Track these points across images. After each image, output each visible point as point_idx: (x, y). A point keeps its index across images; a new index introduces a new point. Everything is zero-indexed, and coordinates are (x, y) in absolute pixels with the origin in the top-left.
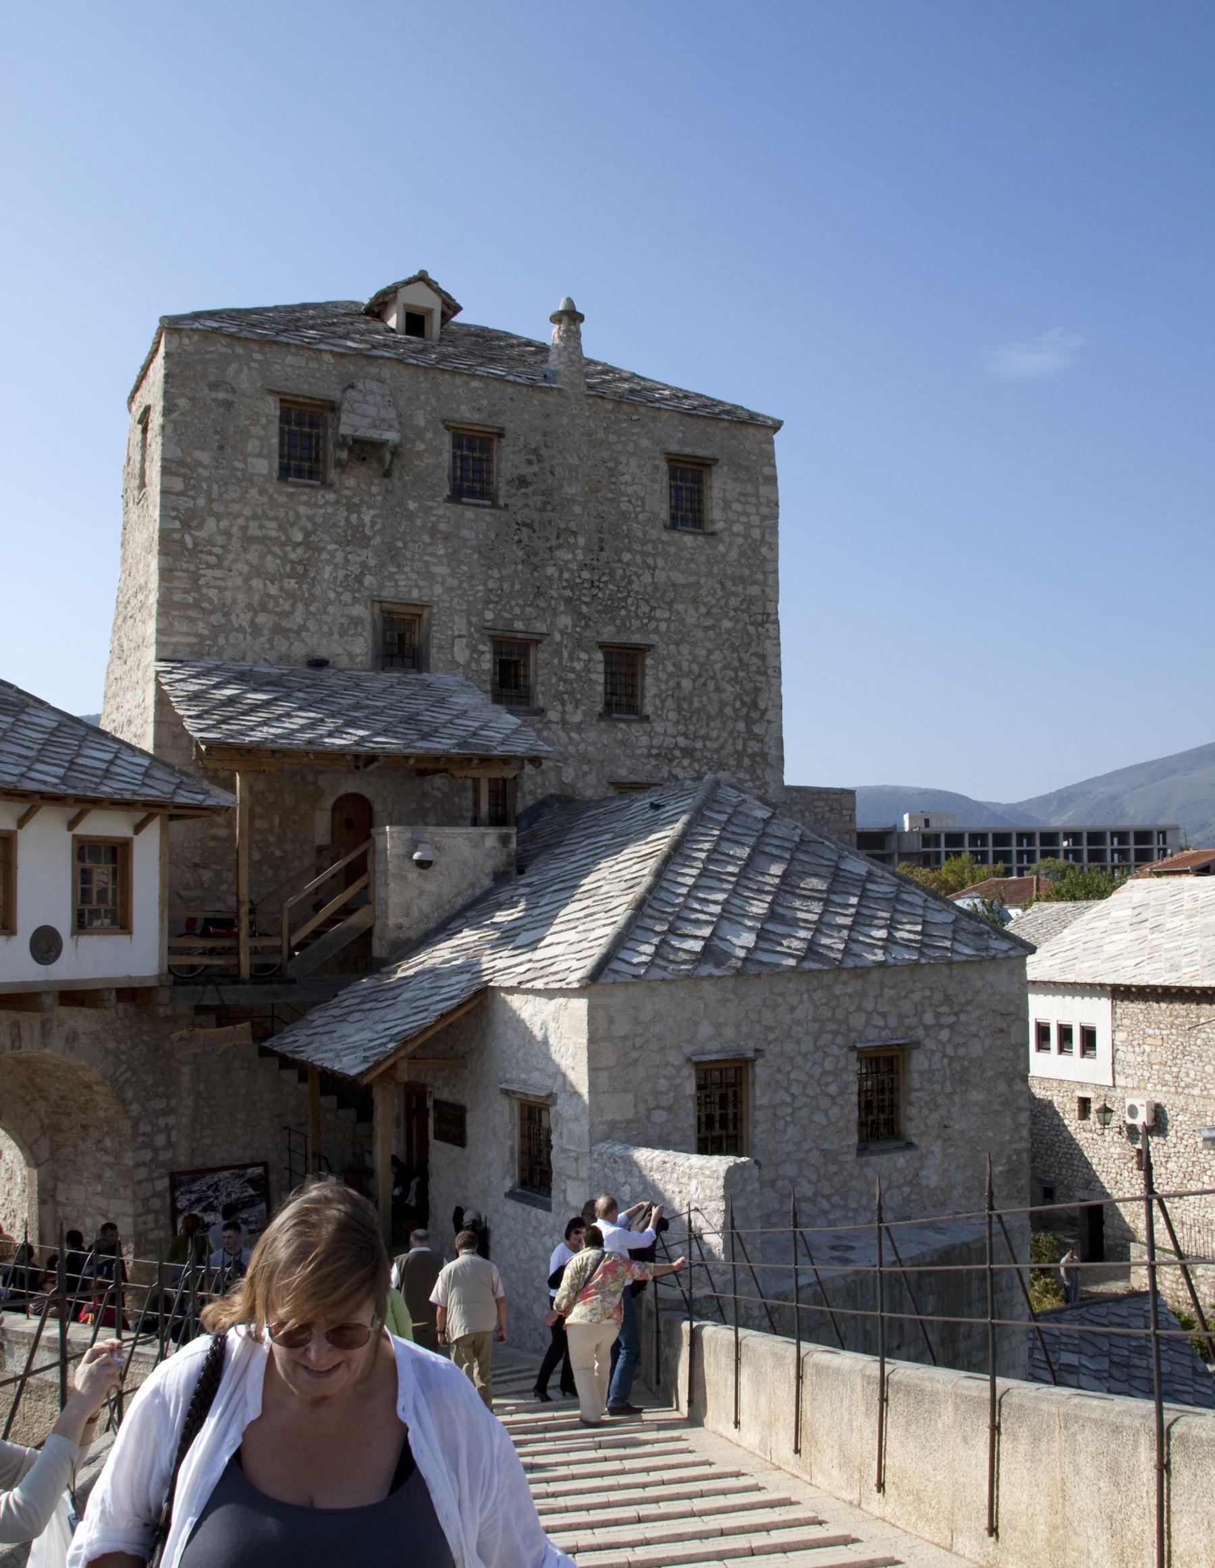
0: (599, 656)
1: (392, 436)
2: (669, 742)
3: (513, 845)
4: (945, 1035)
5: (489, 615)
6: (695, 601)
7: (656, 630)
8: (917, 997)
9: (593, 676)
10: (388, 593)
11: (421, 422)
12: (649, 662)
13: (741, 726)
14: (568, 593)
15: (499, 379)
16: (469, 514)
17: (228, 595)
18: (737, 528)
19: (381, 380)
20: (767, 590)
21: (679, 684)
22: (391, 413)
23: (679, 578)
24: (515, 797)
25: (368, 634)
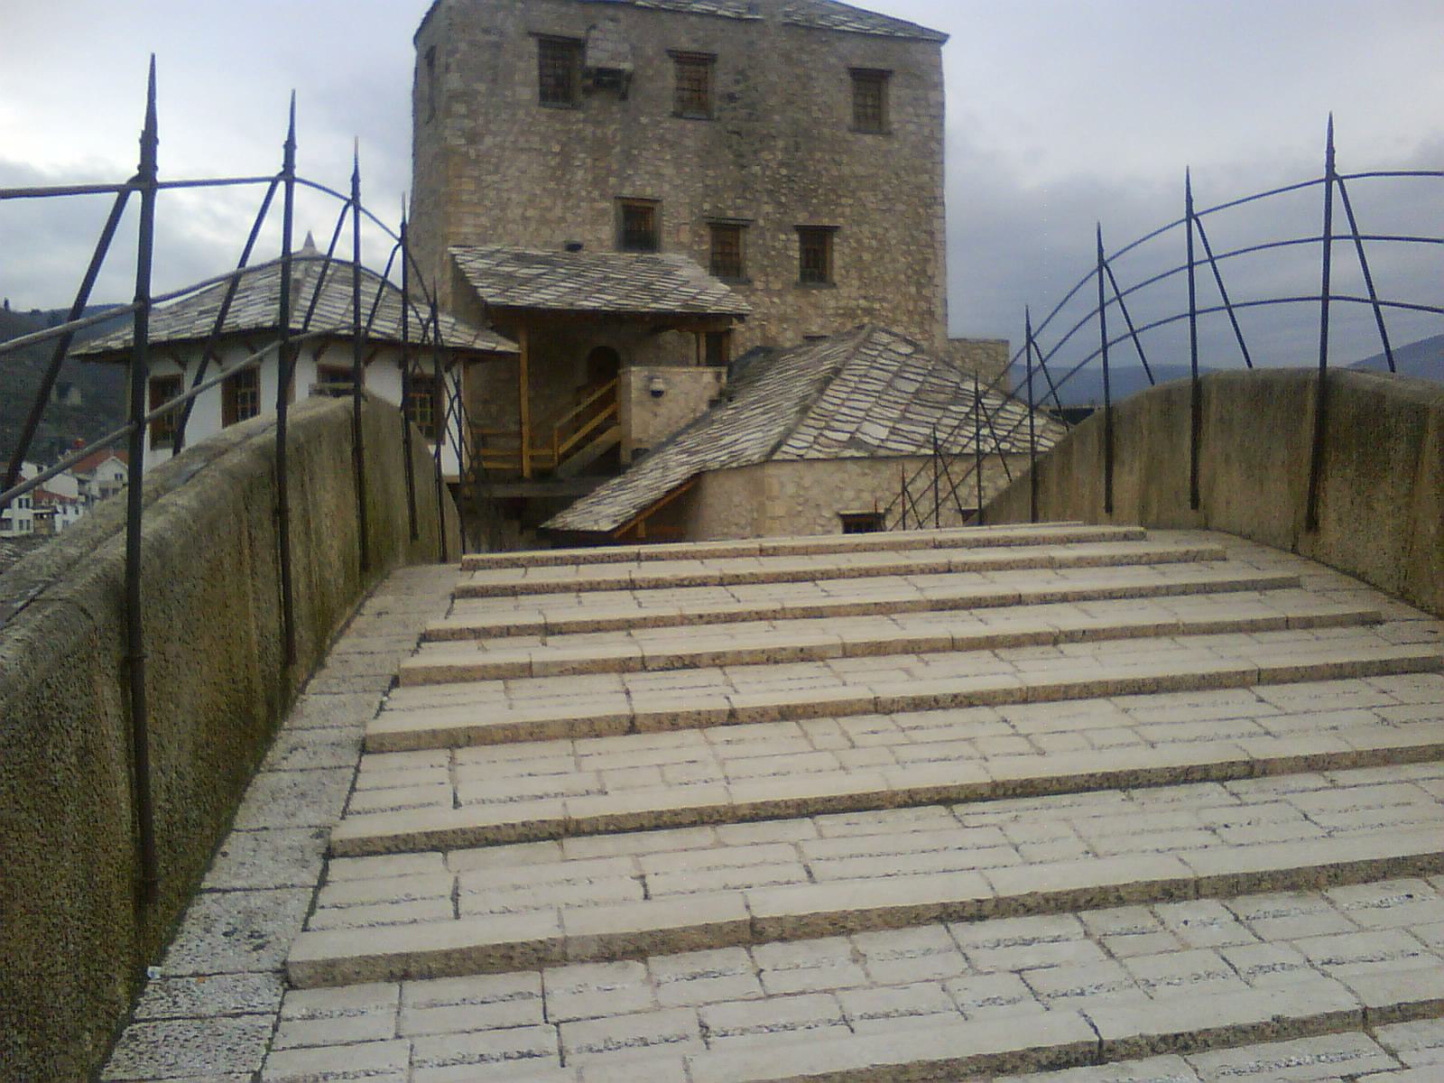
0: (796, 237)
1: (626, 66)
2: (853, 304)
5: (707, 206)
6: (874, 188)
9: (791, 253)
10: (627, 192)
11: (650, 52)
12: (836, 240)
13: (913, 290)
14: (770, 186)
15: (712, 15)
16: (690, 126)
17: (505, 195)
18: (911, 127)
20: (936, 178)
21: (861, 257)
22: (625, 48)
23: (860, 170)
24: (729, 349)
25: (612, 223)
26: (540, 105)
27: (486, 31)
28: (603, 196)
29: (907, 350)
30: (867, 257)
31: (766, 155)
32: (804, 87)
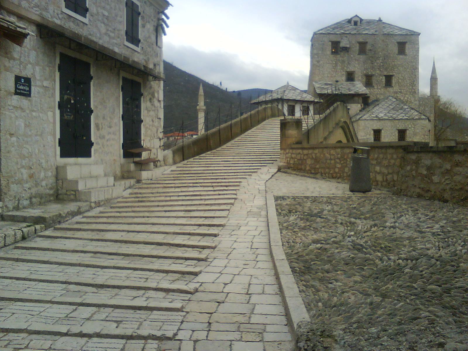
0: (384, 77)
1: (348, 46)
3: (363, 106)
4: (413, 128)
5: (365, 72)
7: (395, 72)
8: (408, 123)
10: (348, 70)
11: (353, 42)
12: (393, 77)
13: (411, 87)
15: (367, 34)
16: (361, 56)
19: (346, 37)
21: (399, 81)
22: (348, 42)
23: (399, 63)
26: (332, 55)
27: (321, 42)
28: (343, 71)
29: (394, 100)
30: (400, 81)
31: (378, 61)
32: (387, 46)
